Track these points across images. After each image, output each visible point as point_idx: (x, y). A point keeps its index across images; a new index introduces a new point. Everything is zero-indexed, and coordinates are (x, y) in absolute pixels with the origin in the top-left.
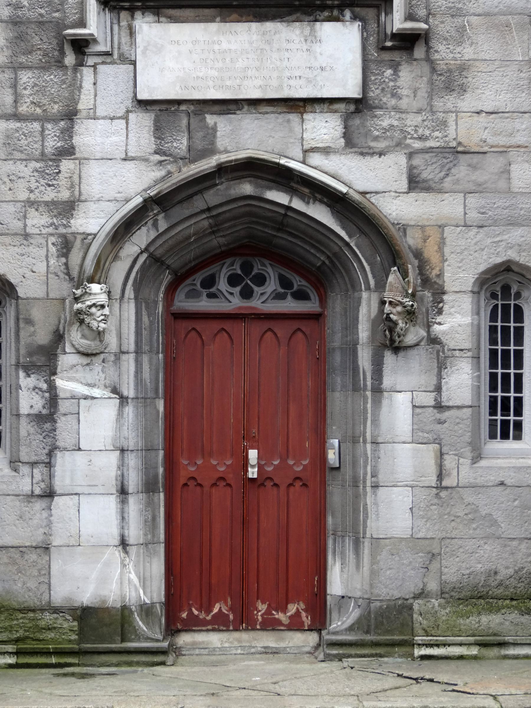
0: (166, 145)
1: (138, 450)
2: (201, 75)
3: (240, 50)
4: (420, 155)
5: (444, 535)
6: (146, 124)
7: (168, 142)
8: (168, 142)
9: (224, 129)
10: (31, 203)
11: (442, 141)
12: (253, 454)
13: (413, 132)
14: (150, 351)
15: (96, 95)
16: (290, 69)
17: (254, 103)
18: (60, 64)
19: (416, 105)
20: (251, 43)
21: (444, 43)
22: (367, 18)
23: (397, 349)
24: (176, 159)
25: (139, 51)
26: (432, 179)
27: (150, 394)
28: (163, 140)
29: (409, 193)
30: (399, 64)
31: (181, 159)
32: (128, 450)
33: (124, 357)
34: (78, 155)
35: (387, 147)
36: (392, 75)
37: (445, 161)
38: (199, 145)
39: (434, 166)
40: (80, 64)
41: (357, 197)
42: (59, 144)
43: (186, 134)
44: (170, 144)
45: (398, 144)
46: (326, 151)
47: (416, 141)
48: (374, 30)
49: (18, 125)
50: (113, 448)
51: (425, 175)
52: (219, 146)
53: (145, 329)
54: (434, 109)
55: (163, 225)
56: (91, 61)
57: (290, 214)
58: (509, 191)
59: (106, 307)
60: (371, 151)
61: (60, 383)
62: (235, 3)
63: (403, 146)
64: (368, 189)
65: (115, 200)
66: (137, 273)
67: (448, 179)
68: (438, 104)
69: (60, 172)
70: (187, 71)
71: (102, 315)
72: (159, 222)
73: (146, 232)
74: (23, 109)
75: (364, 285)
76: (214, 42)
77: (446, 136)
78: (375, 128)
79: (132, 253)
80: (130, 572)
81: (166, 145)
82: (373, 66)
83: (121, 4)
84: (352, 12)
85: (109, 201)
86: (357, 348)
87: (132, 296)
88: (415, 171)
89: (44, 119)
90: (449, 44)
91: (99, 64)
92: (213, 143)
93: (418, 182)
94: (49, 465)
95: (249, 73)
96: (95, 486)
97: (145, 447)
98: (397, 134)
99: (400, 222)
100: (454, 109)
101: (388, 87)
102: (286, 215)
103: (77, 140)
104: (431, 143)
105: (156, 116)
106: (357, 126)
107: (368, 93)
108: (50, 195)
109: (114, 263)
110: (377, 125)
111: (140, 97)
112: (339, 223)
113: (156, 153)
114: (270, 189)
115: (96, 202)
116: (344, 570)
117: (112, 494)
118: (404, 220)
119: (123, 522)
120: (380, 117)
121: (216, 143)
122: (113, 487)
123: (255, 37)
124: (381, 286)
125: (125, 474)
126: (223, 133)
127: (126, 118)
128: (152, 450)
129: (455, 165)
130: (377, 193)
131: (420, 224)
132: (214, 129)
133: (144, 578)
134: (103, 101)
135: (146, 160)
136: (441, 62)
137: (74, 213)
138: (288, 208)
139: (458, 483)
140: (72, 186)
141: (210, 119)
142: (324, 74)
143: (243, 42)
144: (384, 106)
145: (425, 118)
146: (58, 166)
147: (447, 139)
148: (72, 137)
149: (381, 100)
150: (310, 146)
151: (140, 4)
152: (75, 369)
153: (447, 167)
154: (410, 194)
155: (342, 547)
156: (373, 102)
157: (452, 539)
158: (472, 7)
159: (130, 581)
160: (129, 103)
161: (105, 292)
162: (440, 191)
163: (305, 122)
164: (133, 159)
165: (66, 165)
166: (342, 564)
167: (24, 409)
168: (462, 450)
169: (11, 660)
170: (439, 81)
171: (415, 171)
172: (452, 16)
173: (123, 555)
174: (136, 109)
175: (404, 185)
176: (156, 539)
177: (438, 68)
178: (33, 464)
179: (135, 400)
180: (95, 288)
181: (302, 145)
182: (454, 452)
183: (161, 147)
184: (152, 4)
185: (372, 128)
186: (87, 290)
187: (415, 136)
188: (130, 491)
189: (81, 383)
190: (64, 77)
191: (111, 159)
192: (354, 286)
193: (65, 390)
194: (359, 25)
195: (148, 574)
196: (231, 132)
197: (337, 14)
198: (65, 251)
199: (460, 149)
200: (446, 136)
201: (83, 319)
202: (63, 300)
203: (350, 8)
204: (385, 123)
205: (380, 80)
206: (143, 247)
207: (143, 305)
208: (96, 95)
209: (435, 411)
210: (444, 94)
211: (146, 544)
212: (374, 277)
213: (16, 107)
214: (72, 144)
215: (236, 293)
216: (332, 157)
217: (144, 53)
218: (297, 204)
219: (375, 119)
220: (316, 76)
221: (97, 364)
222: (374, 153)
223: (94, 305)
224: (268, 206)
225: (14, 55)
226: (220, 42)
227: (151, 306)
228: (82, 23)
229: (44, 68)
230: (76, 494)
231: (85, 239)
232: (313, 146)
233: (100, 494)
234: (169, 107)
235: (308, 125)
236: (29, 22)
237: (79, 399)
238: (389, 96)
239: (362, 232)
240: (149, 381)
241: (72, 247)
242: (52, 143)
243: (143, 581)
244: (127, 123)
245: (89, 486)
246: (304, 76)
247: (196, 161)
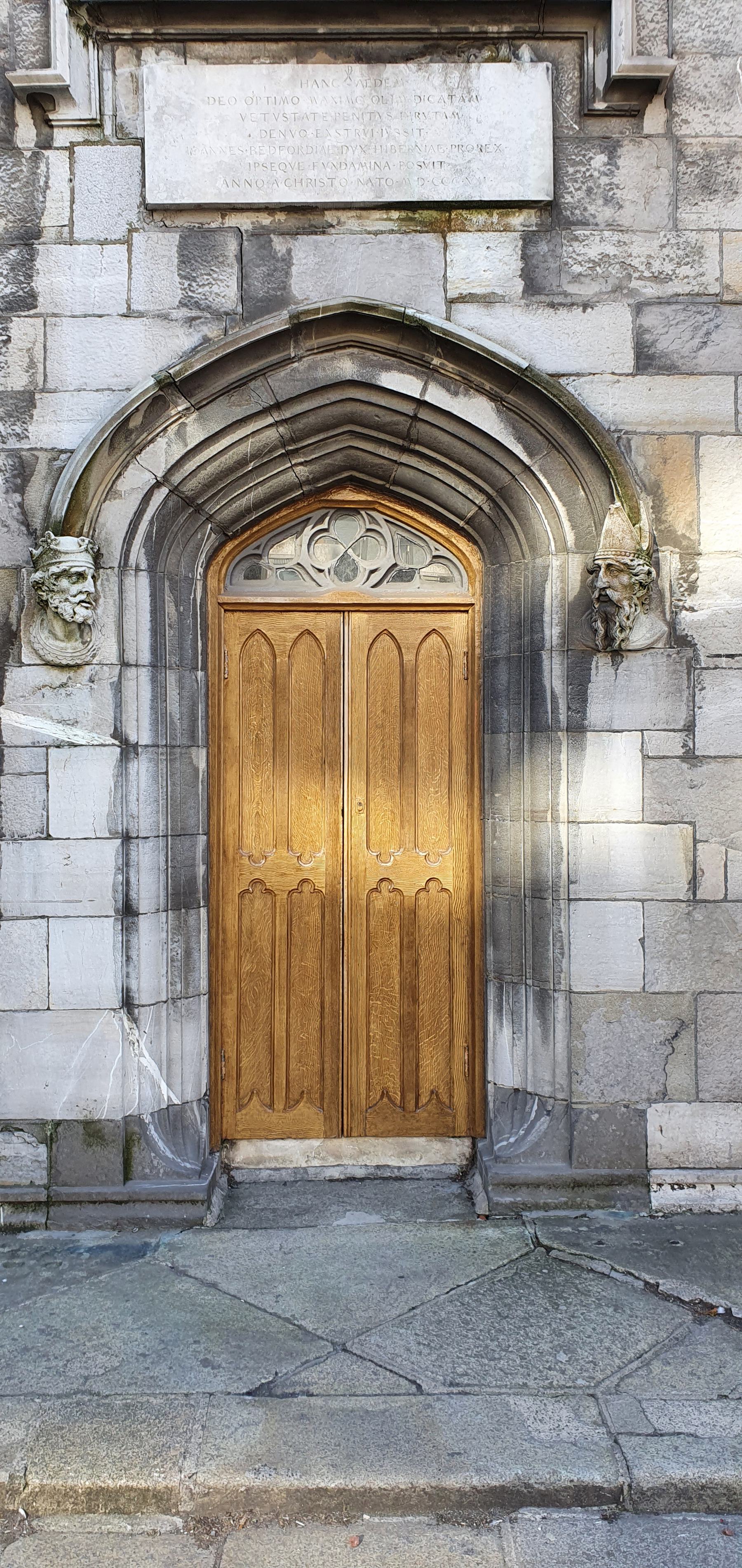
0: (200, 290)
1: (158, 836)
2: (261, 159)
3: (333, 114)
4: (655, 309)
5: (701, 987)
6: (164, 253)
7: (204, 285)
8: (204, 285)
9: (304, 261)
11: (694, 282)
13: (642, 268)
14: (180, 665)
15: (72, 202)
16: (423, 149)
20: (352, 102)
21: (699, 105)
22: (560, 59)
25: (149, 115)
26: (676, 351)
27: (181, 740)
28: (196, 281)
29: (636, 375)
30: (617, 144)
31: (227, 314)
32: (137, 837)
33: (131, 673)
35: (596, 295)
36: (605, 165)
37: (701, 319)
38: (259, 288)
39: (682, 327)
40: (46, 144)
42: (8, 291)
44: (207, 288)
45: (617, 289)
46: (487, 300)
47: (648, 284)
48: (574, 82)
50: (108, 835)
51: (663, 345)
52: (295, 292)
53: (170, 626)
54: (681, 226)
57: (423, 414)
59: (89, 577)
60: (569, 300)
62: (321, 30)
63: (625, 291)
64: (562, 370)
65: (109, 389)
66: (151, 523)
67: (707, 351)
68: (688, 216)
69: (9, 340)
70: (238, 152)
71: (81, 592)
72: (188, 429)
73: (165, 446)
75: (555, 542)
76: (285, 101)
77: (703, 275)
78: (575, 259)
79: (140, 485)
80: (141, 1055)
81: (200, 290)
82: (570, 148)
83: (117, 31)
84: (534, 51)
85: (97, 390)
86: (540, 656)
88: (647, 336)
90: (708, 108)
91: (79, 144)
92: (285, 287)
93: (652, 357)
95: (350, 156)
96: (77, 902)
97: (172, 830)
98: (615, 271)
99: (620, 427)
100: (715, 227)
101: (599, 187)
102: (415, 418)
104: (676, 287)
105: (181, 236)
106: (543, 256)
107: (563, 197)
109: (107, 502)
110: (578, 255)
111: (150, 200)
112: (511, 430)
114: (388, 368)
115: (75, 393)
116: (517, 1042)
117: (107, 917)
118: (628, 424)
119: (127, 965)
120: (584, 241)
121: (290, 286)
122: (109, 904)
123: (359, 91)
125: (133, 880)
126: (302, 269)
127: (127, 242)
128: (184, 835)
129: (717, 327)
130: (578, 375)
131: (657, 430)
132: (287, 260)
133: (169, 1061)
134: (87, 212)
135: (165, 317)
136: (693, 141)
137: (35, 412)
138: (422, 403)
139: (726, 895)
140: (32, 364)
142: (485, 157)
143: (338, 100)
144: (591, 220)
145: (665, 241)
147: (703, 279)
148: (31, 277)
149: (585, 209)
150: (459, 291)
151: (150, 31)
152: (39, 694)
153: (704, 329)
154: (638, 377)
155: (514, 1002)
156: (572, 213)
157: (717, 993)
159: (141, 1069)
160: (133, 215)
161: (87, 550)
163: (449, 248)
164: (141, 315)
166: (514, 1033)
168: (732, 835)
170: (690, 176)
171: (647, 336)
172: (714, 56)
173: (127, 1024)
174: (145, 225)
175: (628, 362)
176: (191, 989)
177: (688, 151)
179: (151, 749)
180: (67, 543)
181: (445, 291)
182: (718, 839)
183: (190, 294)
184: (172, 31)
185: (570, 260)
186: (52, 546)
187: (647, 274)
189: (51, 718)
190: (15, 169)
191: (100, 316)
193: (16, 730)
194: (548, 69)
195: (176, 1053)
196: (317, 267)
197: (506, 54)
198: (19, 481)
199: (727, 297)
200: (703, 275)
201: (47, 601)
202: (17, 569)
203: (531, 42)
204: (594, 251)
205: (584, 173)
206: (160, 474)
207: (167, 584)
208: (72, 202)
209: (685, 766)
210: (698, 198)
211: (172, 999)
212: (574, 527)
214: (32, 289)
215: (329, 570)
217: (158, 119)
218: (436, 395)
219: (575, 244)
220: (469, 161)
221: (79, 685)
222: (573, 304)
223: (65, 573)
224: (384, 401)
226: (295, 100)
230: (43, 917)
231: (55, 459)
232: (465, 293)
233: (86, 917)
237: (48, 747)
238: (600, 202)
239: (554, 446)
240: (178, 716)
241: (32, 475)
243: (167, 1066)
244: (130, 251)
245: (67, 902)
246: (447, 161)
247: (255, 319)
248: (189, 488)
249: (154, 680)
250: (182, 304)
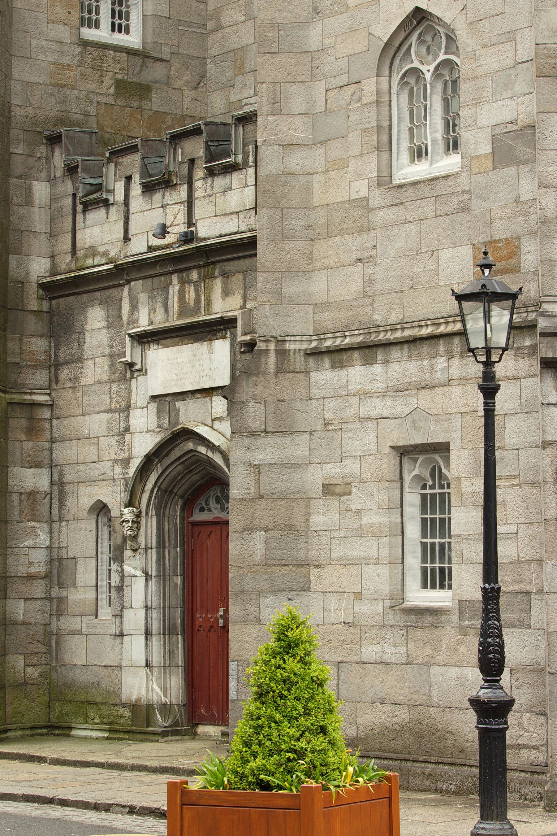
10: (115, 461)
17: (193, 392)
34: (131, 431)
40: (132, 377)
43: (168, 415)
49: (111, 415)
61: (126, 567)
69: (125, 442)
74: (113, 406)
87: (154, 513)
103: (131, 422)
113: (158, 427)
127: (147, 407)
135: (154, 431)
137: (130, 465)
141: (178, 404)
146: (124, 438)
188: (153, 633)
213: (111, 405)
216: (223, 422)
225: (110, 375)
229: (120, 381)
234: (162, 398)
235: (214, 404)
242: (123, 425)
248: (163, 486)
249: (158, 553)
250: (158, 427)
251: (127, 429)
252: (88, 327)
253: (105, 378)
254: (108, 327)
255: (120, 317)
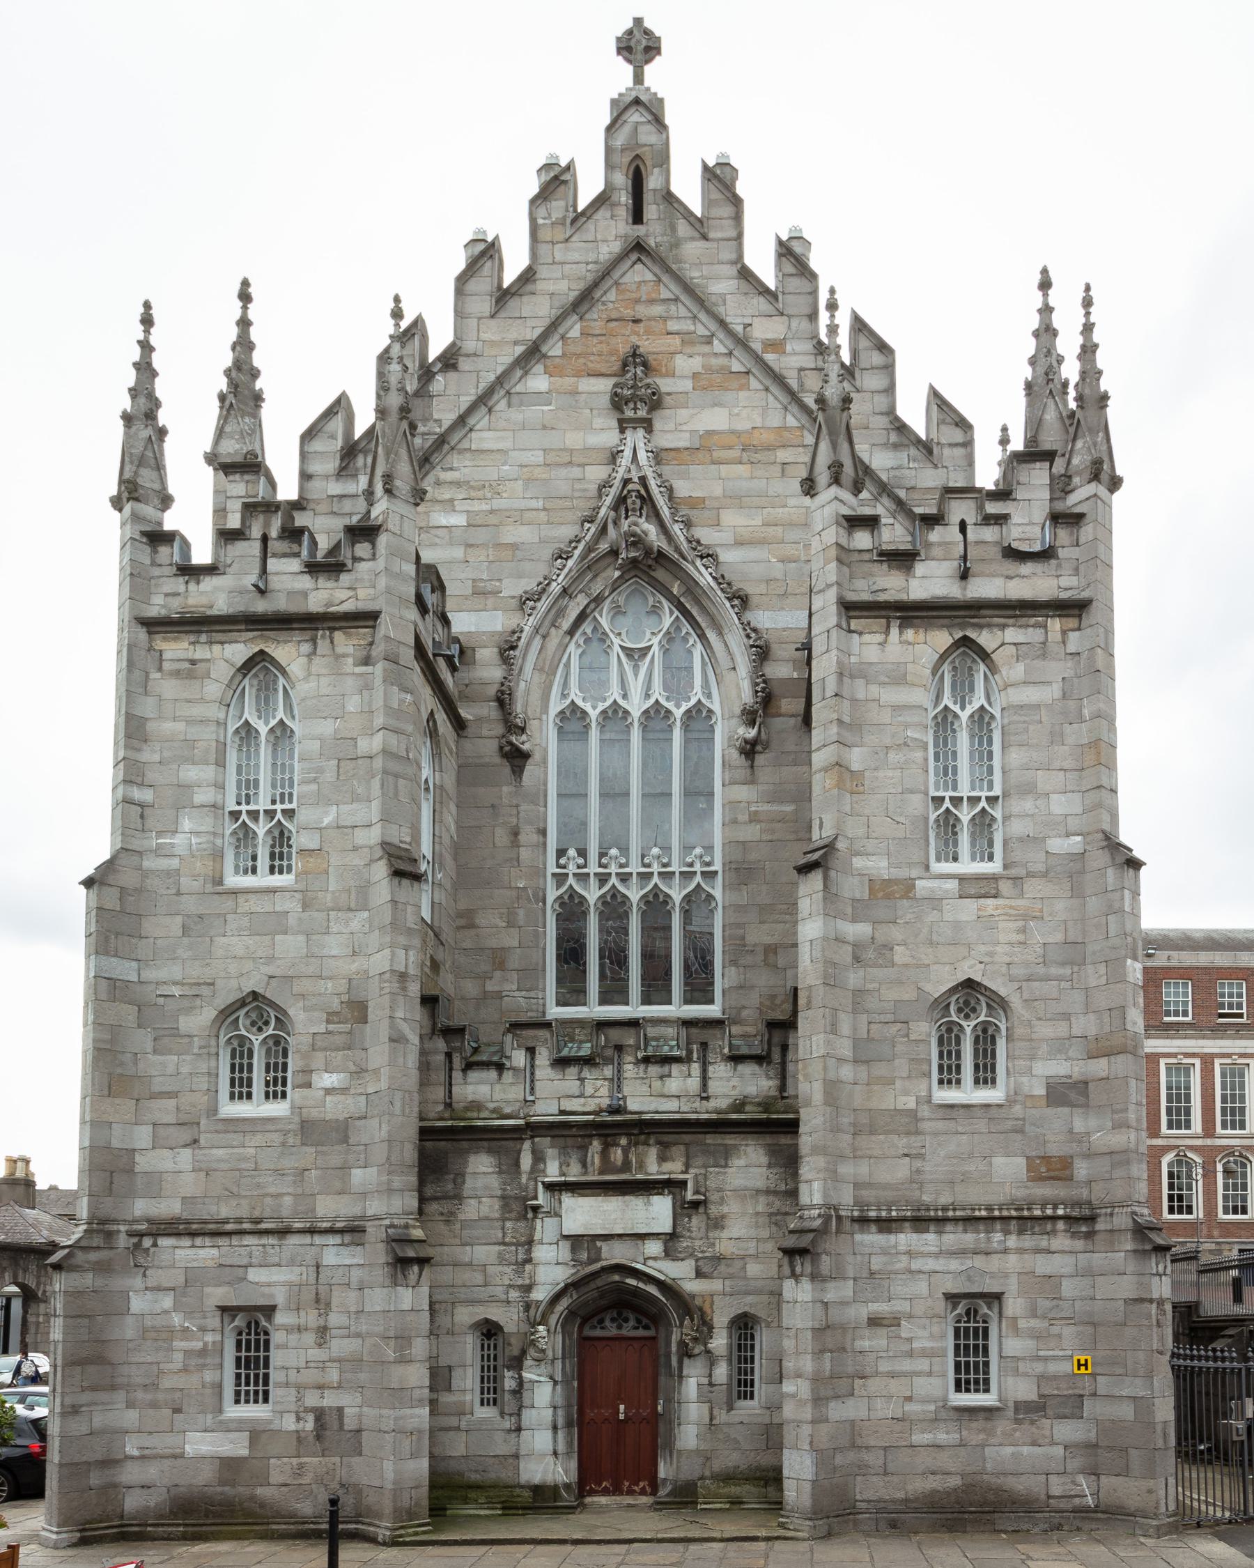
10: (510, 1286)
12: (622, 1407)
17: (620, 1236)
18: (526, 1219)
19: (700, 1235)
23: (690, 1356)
24: (582, 1263)
38: (593, 1256)
40: (535, 1217)
41: (669, 1281)
46: (655, 1259)
55: (575, 1297)
56: (540, 1216)
58: (745, 1278)
61: (525, 1375)
68: (711, 1235)
74: (507, 1240)
89: (517, 1244)
94: (519, 1415)
108: (520, 1282)
124: (681, 1325)
127: (557, 1243)
141: (598, 1244)
158: (727, 1187)
162: (712, 1278)
165: (528, 1267)
167: (507, 1388)
169: (500, 1512)
175: (693, 1275)
178: (511, 1415)
192: (670, 1324)
218: (641, 1285)
227: (571, 1335)
228: (536, 1198)
229: (517, 1220)
236: (510, 1197)
243: (566, 1472)
251: (529, 1260)
252: (470, 1169)
253: (497, 1215)
254: (500, 1173)
255: (517, 1164)
